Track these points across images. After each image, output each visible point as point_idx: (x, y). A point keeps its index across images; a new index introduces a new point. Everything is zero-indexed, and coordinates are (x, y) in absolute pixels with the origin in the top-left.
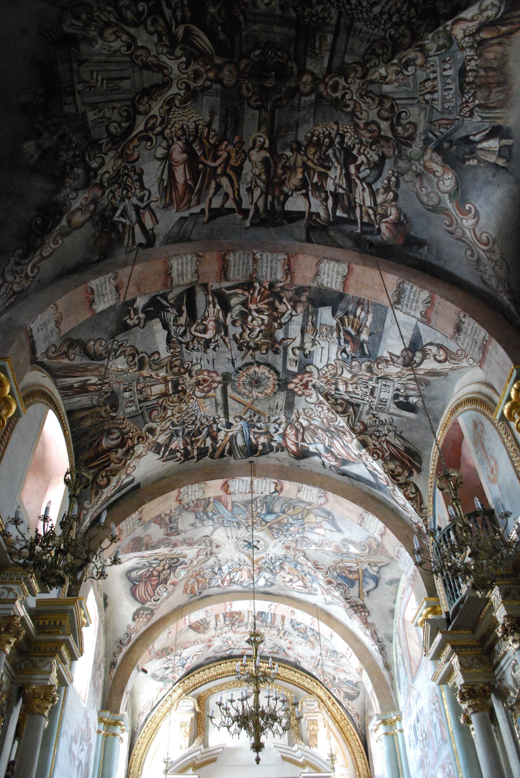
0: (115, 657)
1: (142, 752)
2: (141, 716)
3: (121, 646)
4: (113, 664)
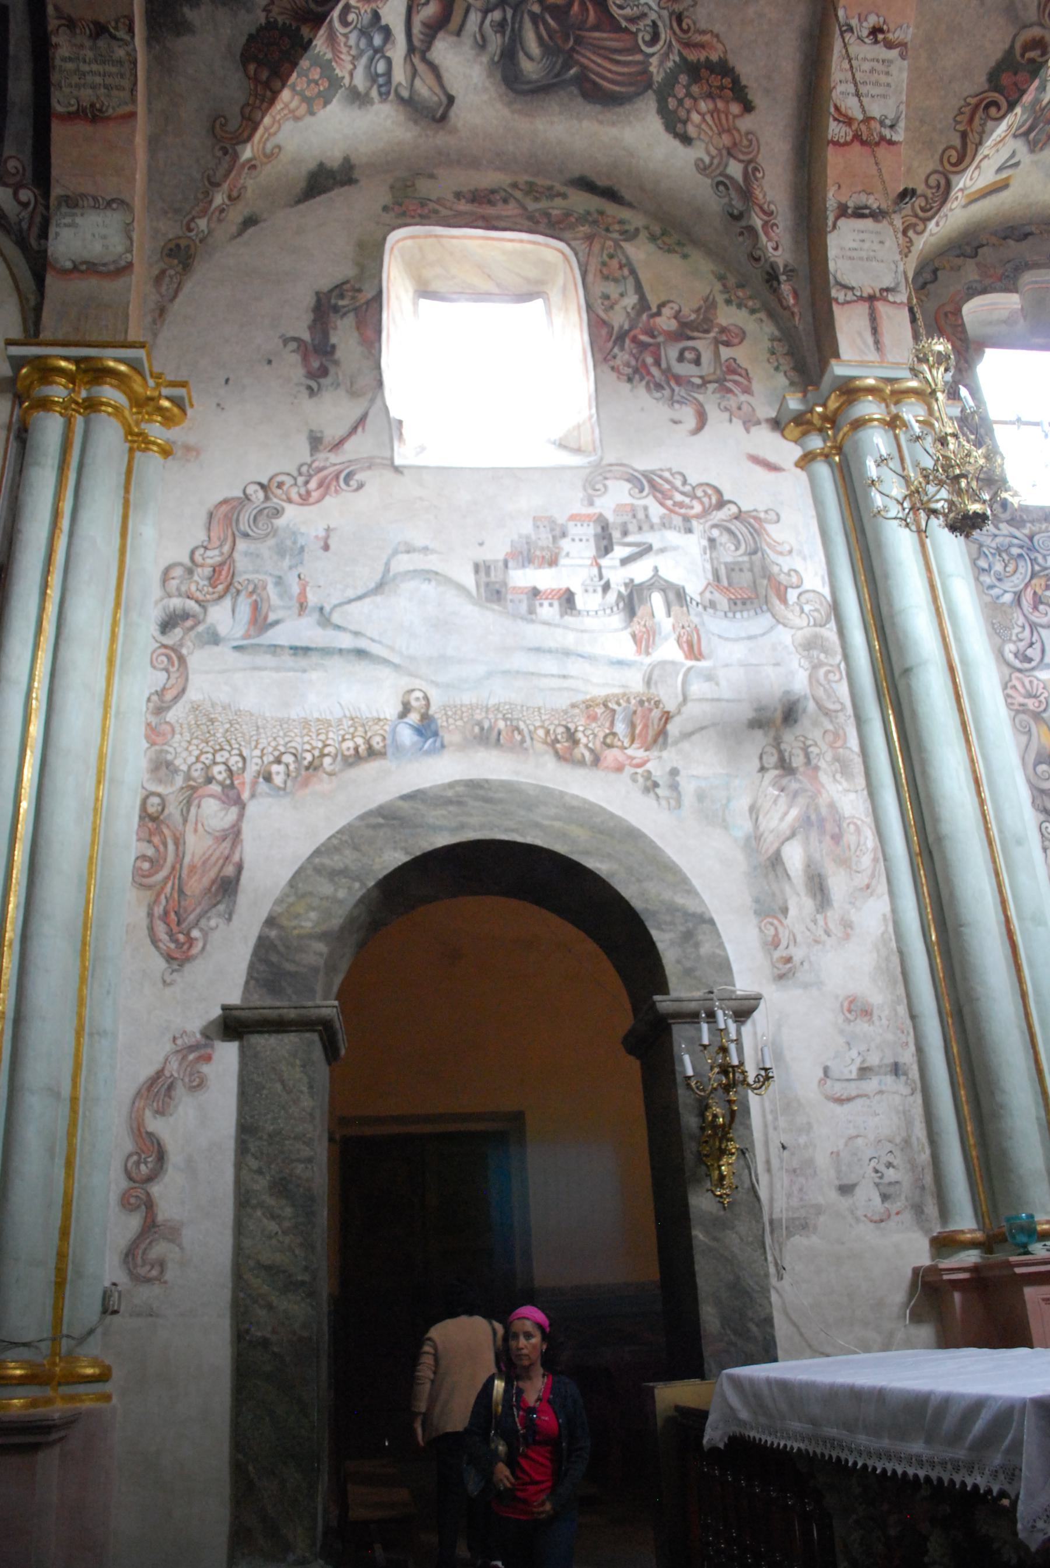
0: (757, 260)
3: (743, 223)
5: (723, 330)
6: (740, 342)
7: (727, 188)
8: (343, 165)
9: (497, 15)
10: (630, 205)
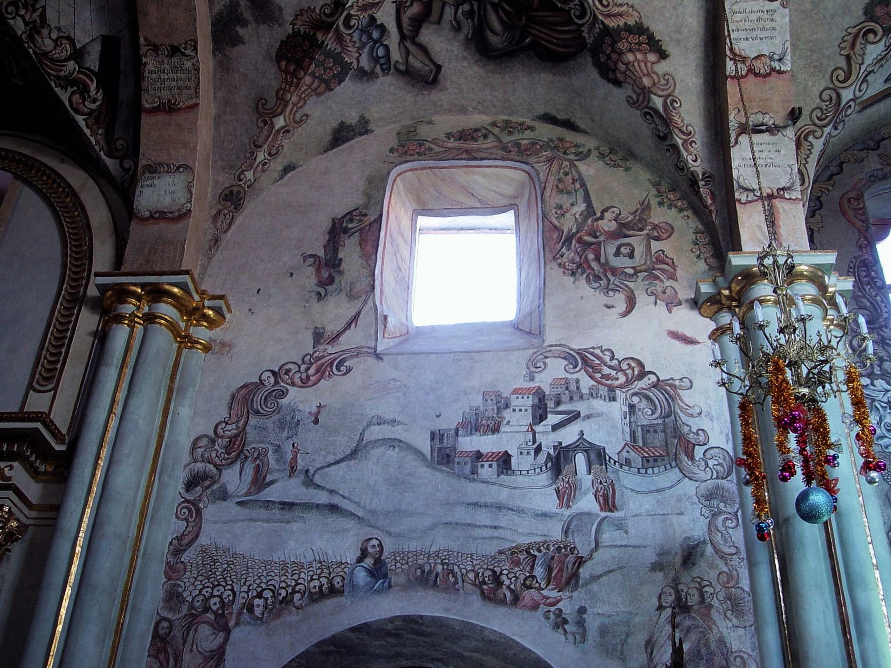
0: (682, 170)
3: (668, 142)
5: (655, 227)
6: (669, 237)
7: (653, 117)
8: (359, 121)
9: (466, 7)
10: (584, 132)
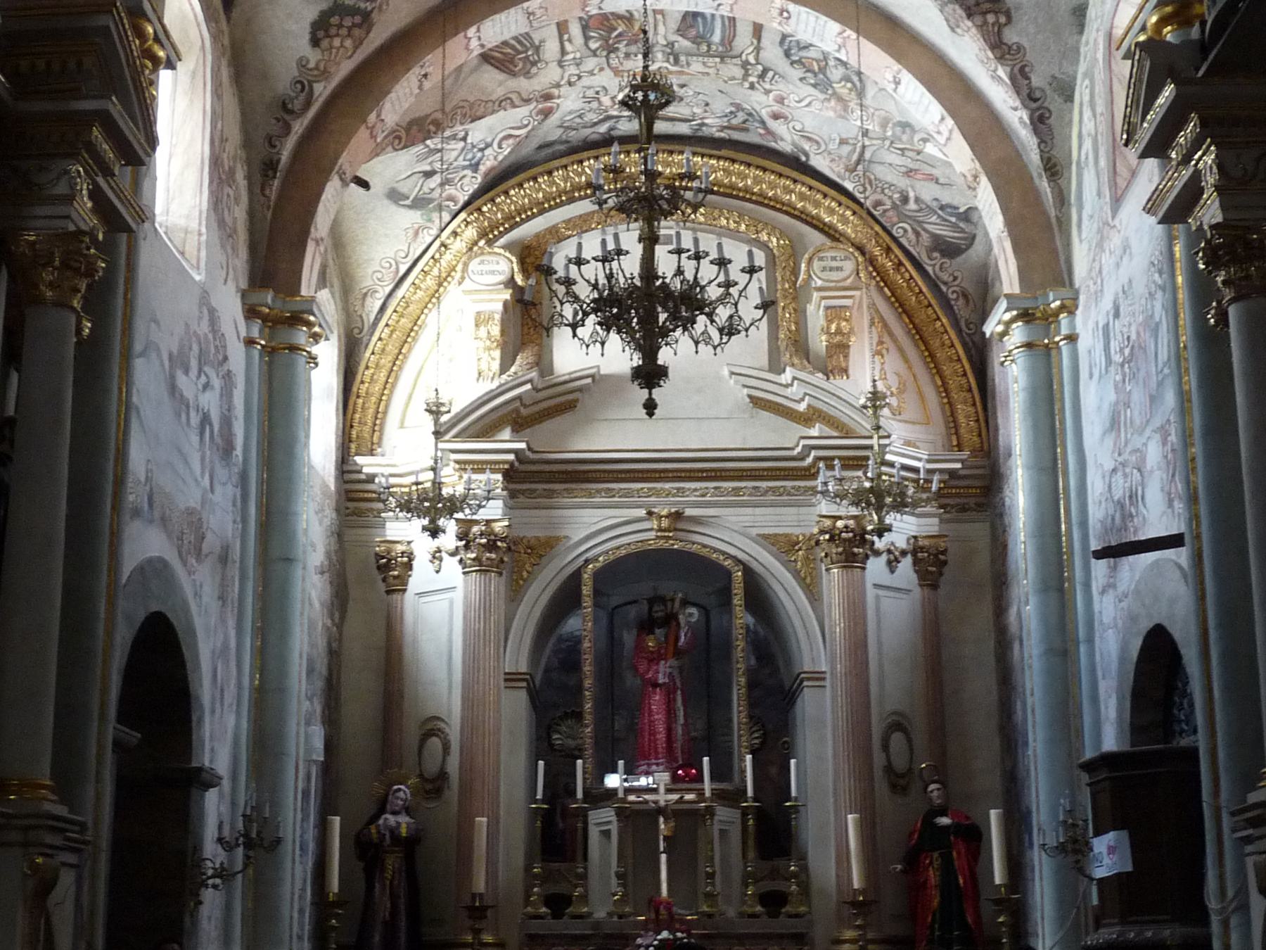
1: (377, 388)
2: (369, 300)
3: (287, 117)
4: (270, 166)
10: (228, 19)
